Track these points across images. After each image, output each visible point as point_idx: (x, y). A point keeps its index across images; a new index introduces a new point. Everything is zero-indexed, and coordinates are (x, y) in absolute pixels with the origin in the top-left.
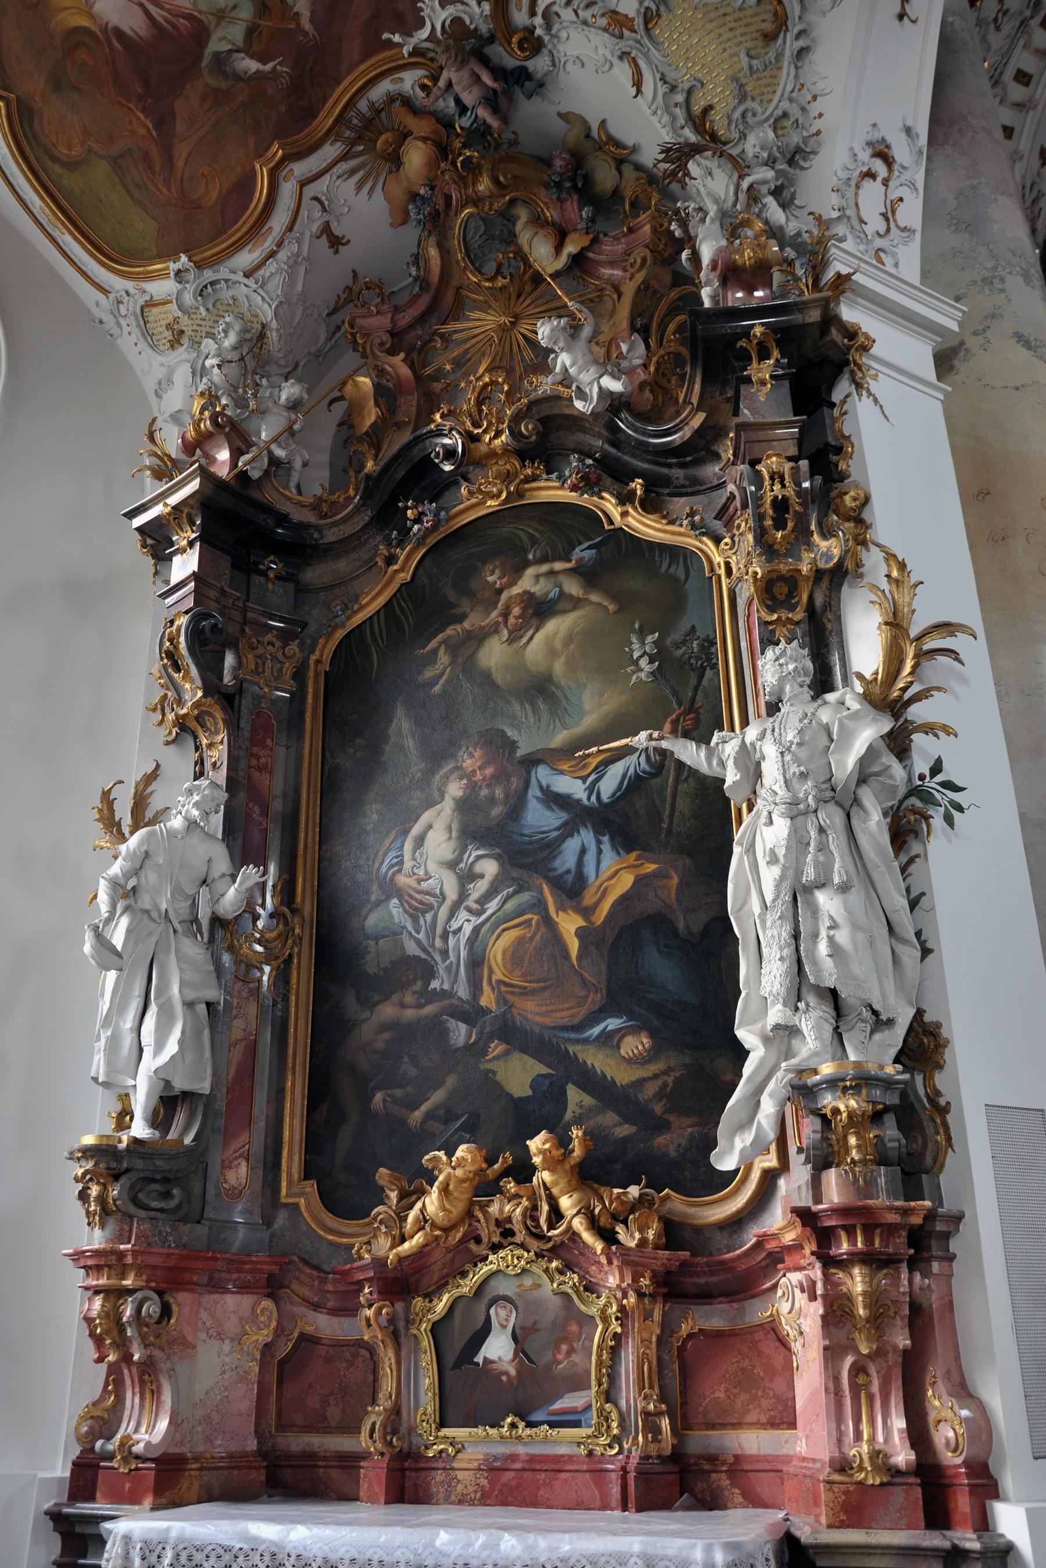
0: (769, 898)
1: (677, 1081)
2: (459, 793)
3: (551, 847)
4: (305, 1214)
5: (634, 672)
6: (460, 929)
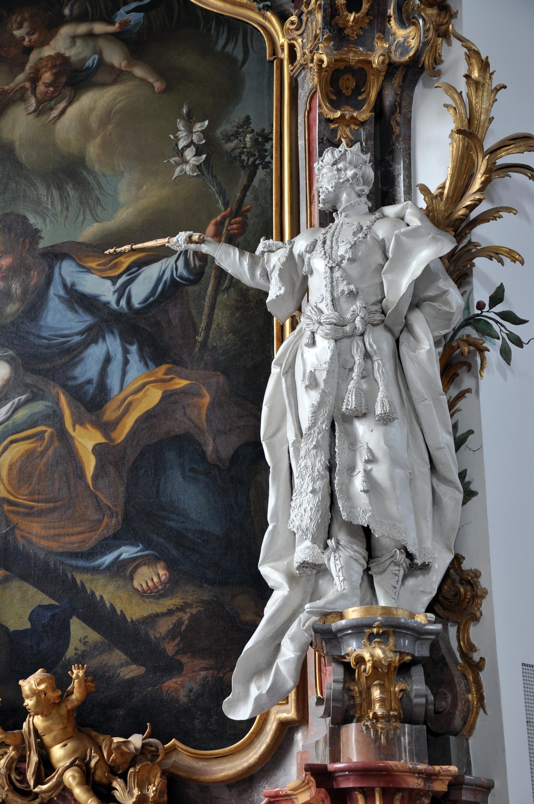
0: (305, 424)
1: (193, 618)
5: (177, 164)
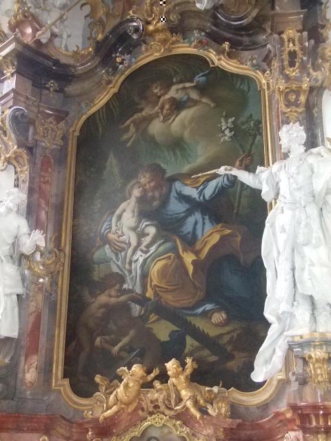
0: (281, 250)
1: (238, 335)
2: (139, 195)
3: (181, 221)
4: (63, 394)
5: (222, 137)
6: (137, 260)
